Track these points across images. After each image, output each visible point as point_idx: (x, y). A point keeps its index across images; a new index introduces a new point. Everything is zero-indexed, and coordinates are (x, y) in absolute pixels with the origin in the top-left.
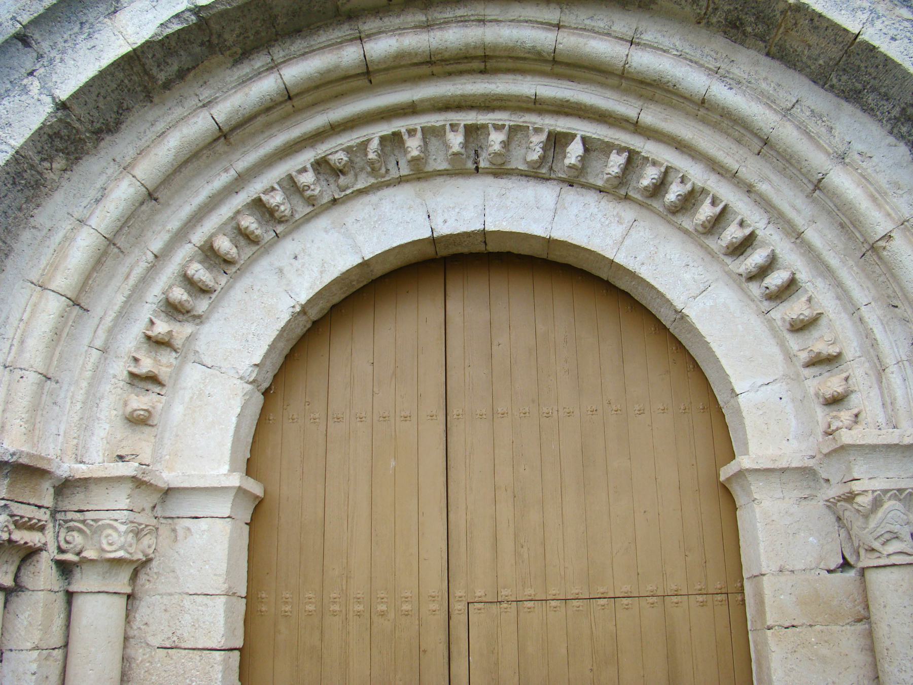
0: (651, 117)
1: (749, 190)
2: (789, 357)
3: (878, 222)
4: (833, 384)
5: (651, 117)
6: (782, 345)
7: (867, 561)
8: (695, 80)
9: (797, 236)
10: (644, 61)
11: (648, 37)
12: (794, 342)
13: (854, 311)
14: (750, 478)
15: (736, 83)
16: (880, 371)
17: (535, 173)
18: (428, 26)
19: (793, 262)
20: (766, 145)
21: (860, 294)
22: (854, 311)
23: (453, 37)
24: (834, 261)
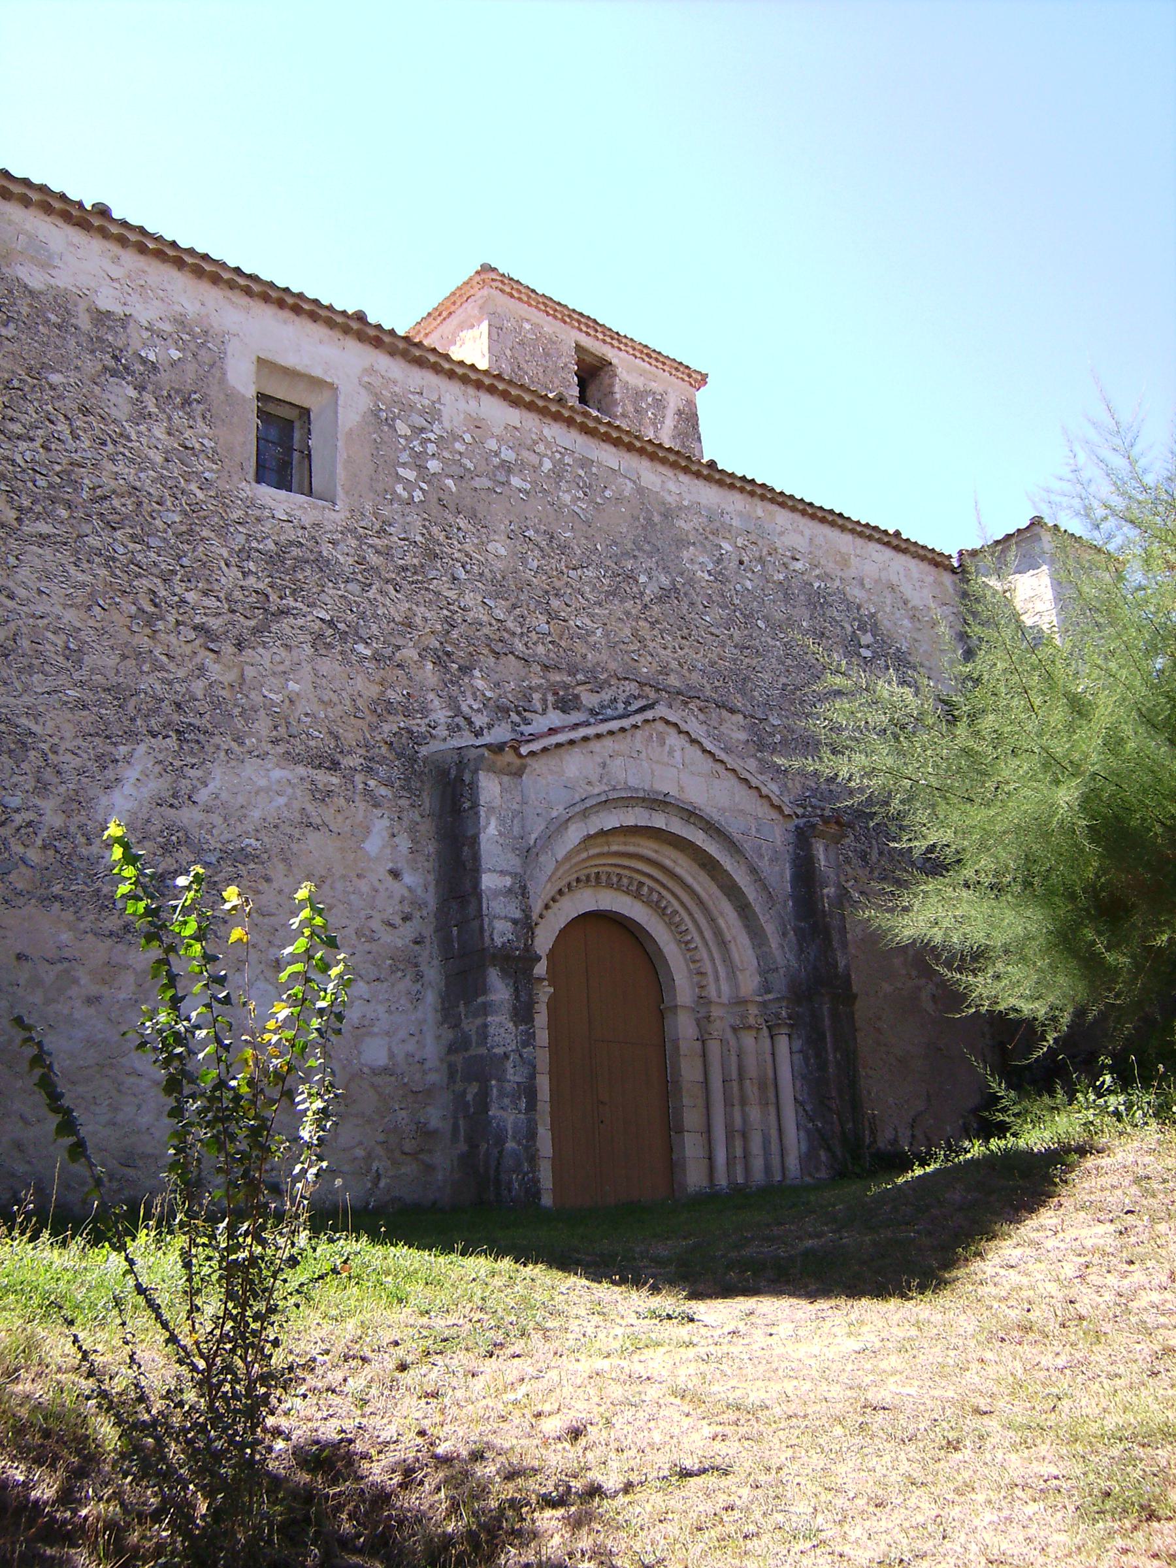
0: (670, 884)
1: (690, 914)
2: (690, 970)
3: (728, 937)
4: (704, 983)
5: (670, 884)
6: (688, 965)
7: (706, 1036)
8: (689, 880)
9: (701, 933)
10: (678, 870)
11: (680, 862)
12: (692, 966)
13: (713, 960)
14: (679, 1011)
15: (699, 882)
16: (717, 979)
17: (628, 892)
18: (625, 844)
19: (698, 941)
20: (700, 902)
21: (716, 955)
22: (713, 960)
23: (631, 849)
24: (710, 944)
